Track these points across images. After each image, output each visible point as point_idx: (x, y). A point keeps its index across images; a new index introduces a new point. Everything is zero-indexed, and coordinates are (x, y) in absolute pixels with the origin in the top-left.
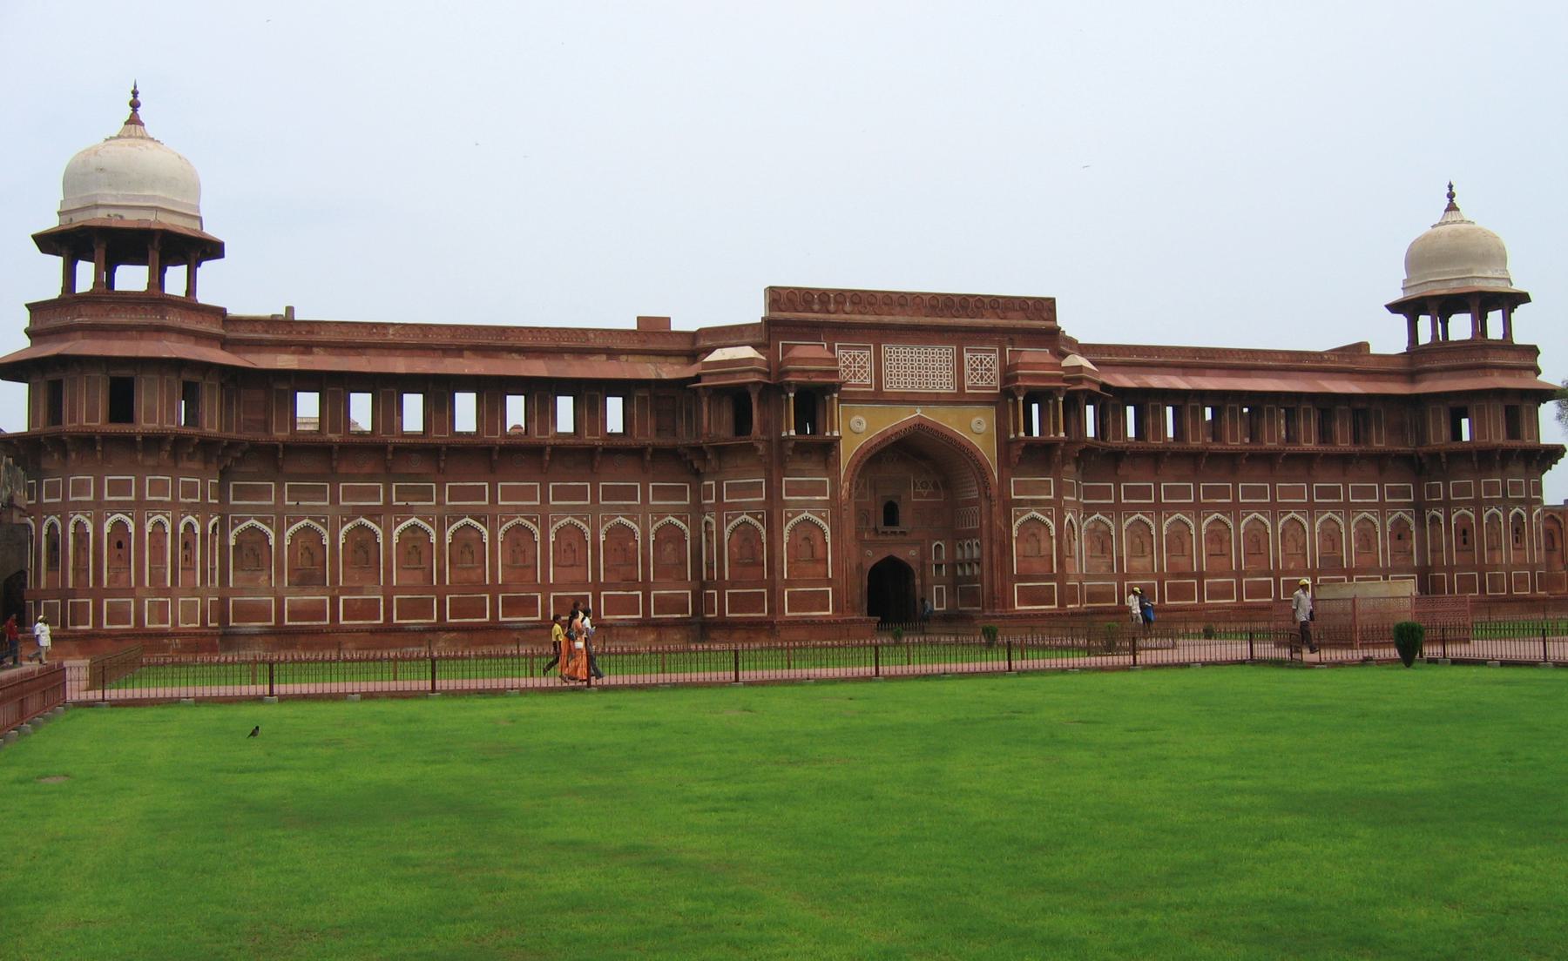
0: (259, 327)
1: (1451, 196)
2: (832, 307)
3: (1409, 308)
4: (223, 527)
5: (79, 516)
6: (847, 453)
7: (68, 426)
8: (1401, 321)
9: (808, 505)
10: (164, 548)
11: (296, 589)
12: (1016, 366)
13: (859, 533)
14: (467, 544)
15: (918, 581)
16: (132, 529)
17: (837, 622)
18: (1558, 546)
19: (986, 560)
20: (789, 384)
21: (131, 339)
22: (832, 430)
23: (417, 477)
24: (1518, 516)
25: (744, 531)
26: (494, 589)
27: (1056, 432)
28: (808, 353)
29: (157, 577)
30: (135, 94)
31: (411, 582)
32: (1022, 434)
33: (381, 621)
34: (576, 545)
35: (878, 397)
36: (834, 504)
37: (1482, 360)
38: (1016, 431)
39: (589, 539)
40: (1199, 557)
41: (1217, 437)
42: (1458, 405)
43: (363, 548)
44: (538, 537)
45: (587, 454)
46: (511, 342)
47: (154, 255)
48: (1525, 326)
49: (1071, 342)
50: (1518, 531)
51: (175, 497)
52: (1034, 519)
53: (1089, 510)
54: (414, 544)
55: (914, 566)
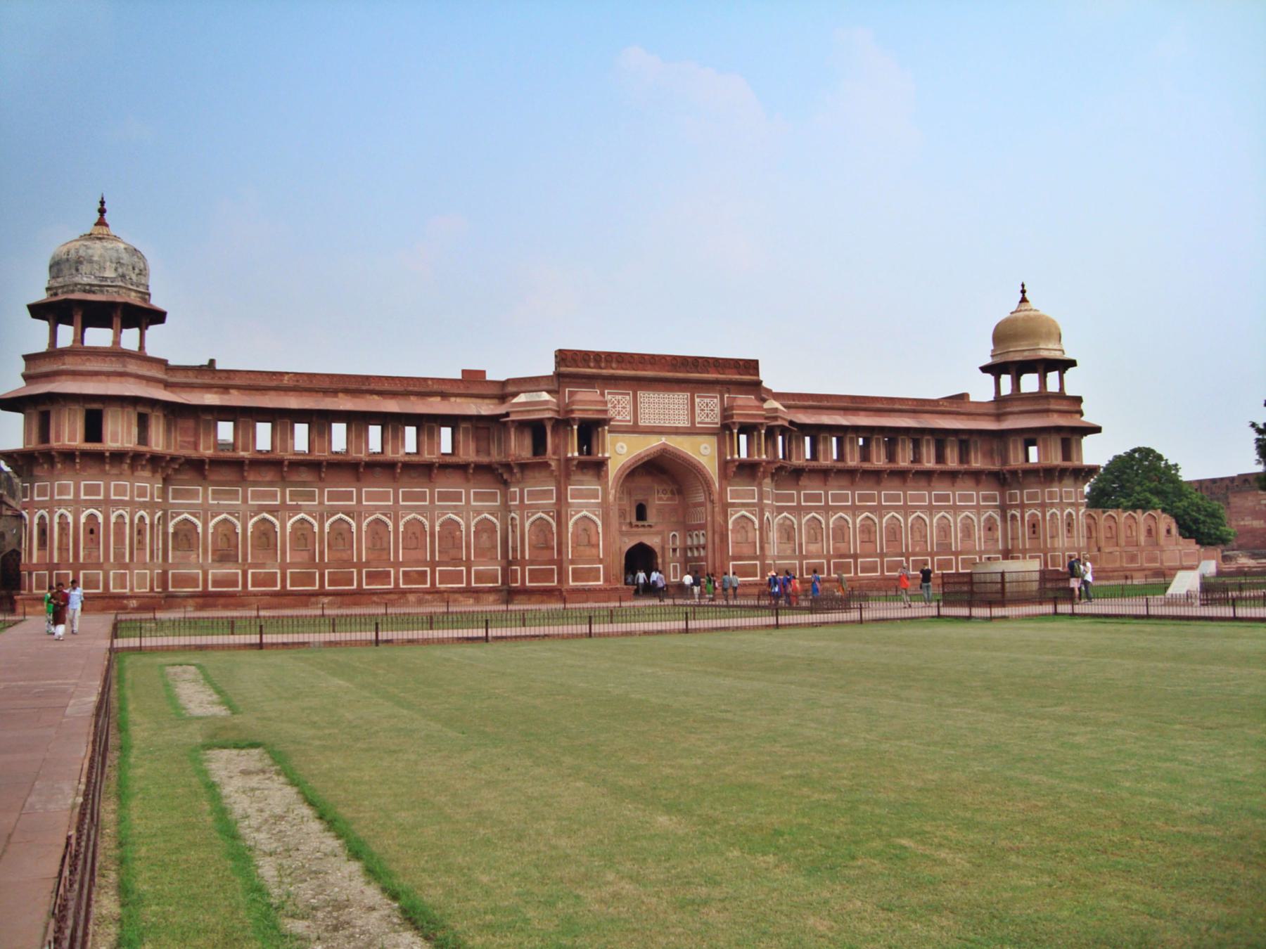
0: (190, 373)
1: (1023, 292)
2: (603, 365)
3: (995, 369)
4: (164, 520)
5: (63, 511)
6: (614, 468)
7: (54, 444)
8: (990, 378)
9: (586, 506)
10: (123, 533)
11: (217, 564)
12: (732, 408)
13: (621, 524)
14: (341, 534)
15: (660, 561)
16: (101, 519)
17: (606, 590)
18: (1094, 534)
19: (710, 546)
20: (574, 419)
21: (100, 381)
22: (603, 452)
23: (304, 484)
24: (1070, 515)
25: (541, 525)
26: (359, 565)
27: (759, 453)
28: (586, 401)
29: (119, 555)
30: (102, 203)
31: (299, 560)
32: (736, 456)
33: (278, 588)
34: (418, 534)
35: (635, 429)
36: (604, 505)
37: (1046, 407)
38: (732, 454)
39: (428, 529)
40: (855, 545)
41: (865, 456)
42: (1030, 437)
43: (265, 536)
44: (391, 528)
46: (372, 387)
47: (117, 321)
48: (1073, 383)
49: (768, 391)
50: (1069, 525)
51: (132, 497)
52: (743, 516)
53: (780, 510)
54: (302, 535)
55: (657, 550)
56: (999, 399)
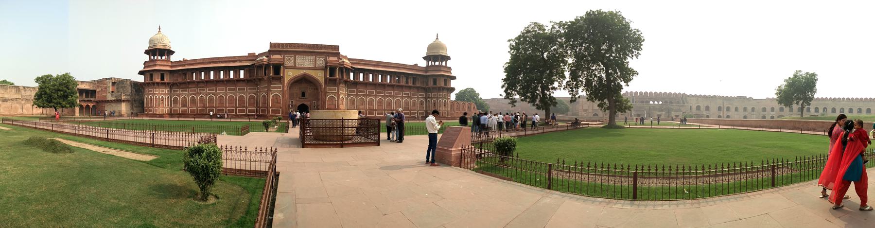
6: (287, 80)
13: (290, 98)
14: (211, 99)
35: (295, 68)
45: (237, 81)
48: (449, 64)
56: (428, 66)
